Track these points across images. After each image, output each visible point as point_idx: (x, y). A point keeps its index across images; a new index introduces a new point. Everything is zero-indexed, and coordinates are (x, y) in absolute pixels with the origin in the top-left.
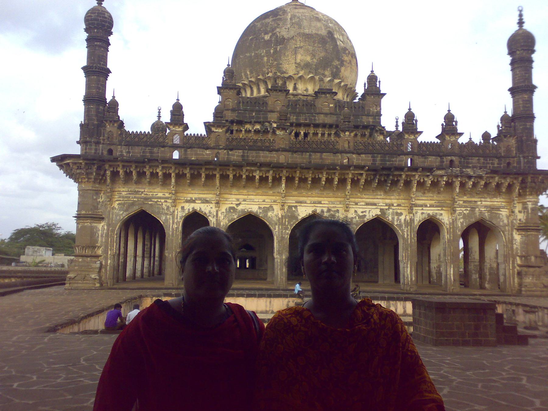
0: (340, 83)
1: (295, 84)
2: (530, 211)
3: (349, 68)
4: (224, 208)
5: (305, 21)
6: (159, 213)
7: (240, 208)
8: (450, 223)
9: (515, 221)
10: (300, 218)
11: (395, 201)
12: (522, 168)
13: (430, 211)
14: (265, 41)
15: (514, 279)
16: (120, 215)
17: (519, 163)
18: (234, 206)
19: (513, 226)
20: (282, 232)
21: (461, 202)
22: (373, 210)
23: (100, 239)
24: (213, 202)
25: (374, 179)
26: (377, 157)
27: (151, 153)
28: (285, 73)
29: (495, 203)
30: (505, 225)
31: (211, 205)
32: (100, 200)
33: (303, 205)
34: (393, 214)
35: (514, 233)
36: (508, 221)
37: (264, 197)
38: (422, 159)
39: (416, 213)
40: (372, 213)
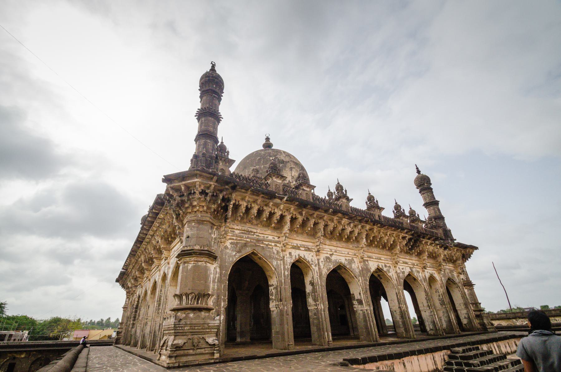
4: (322, 257)
6: (270, 257)
7: (333, 258)
10: (372, 271)
18: (328, 255)
23: (211, 285)
24: (314, 250)
31: (312, 254)
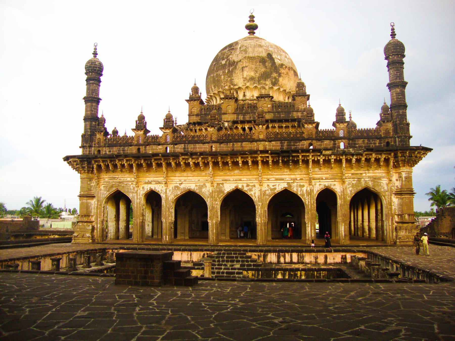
0: (279, 89)
1: (244, 93)
2: (404, 179)
3: (287, 78)
5: (250, 48)
7: (182, 186)
8: (341, 191)
9: (393, 188)
10: (226, 192)
11: (299, 176)
12: (397, 145)
13: (326, 183)
15: (393, 232)
17: (395, 142)
18: (178, 185)
19: (391, 191)
20: (213, 203)
21: (350, 175)
22: (281, 184)
25: (279, 159)
26: (284, 143)
27: (123, 150)
28: (236, 85)
29: (377, 174)
30: (385, 191)
32: (93, 184)
33: (228, 182)
34: (297, 186)
35: (392, 197)
36: (388, 188)
37: (199, 178)
38: (319, 143)
39: (315, 185)
40: (280, 187)
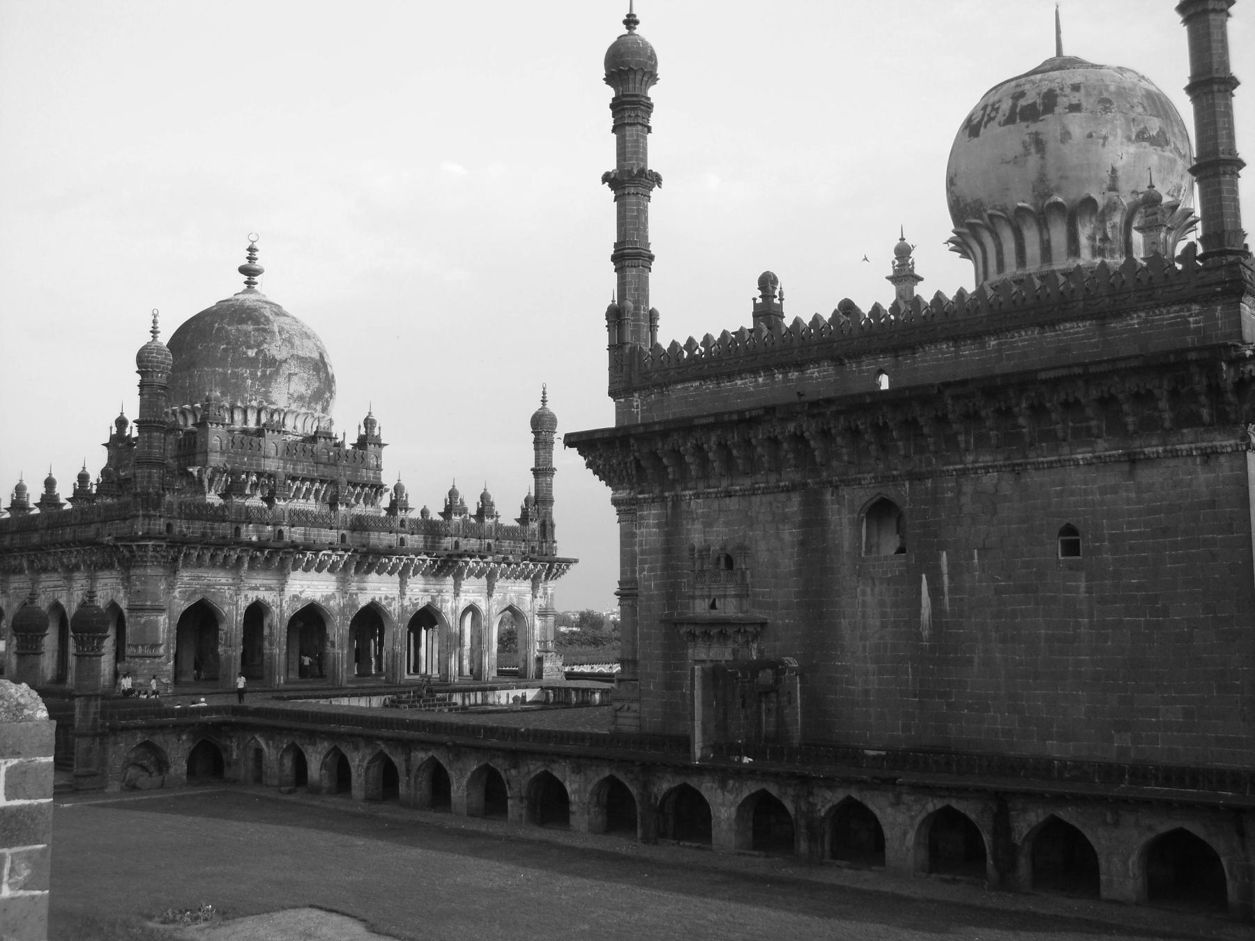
6: (222, 603)
7: (303, 596)
14: (249, 359)
16: (179, 606)
